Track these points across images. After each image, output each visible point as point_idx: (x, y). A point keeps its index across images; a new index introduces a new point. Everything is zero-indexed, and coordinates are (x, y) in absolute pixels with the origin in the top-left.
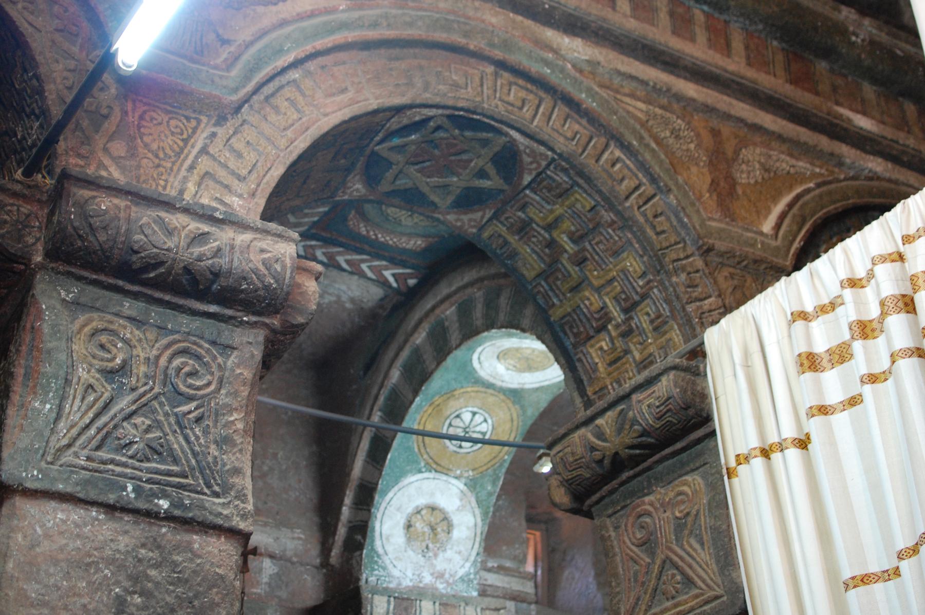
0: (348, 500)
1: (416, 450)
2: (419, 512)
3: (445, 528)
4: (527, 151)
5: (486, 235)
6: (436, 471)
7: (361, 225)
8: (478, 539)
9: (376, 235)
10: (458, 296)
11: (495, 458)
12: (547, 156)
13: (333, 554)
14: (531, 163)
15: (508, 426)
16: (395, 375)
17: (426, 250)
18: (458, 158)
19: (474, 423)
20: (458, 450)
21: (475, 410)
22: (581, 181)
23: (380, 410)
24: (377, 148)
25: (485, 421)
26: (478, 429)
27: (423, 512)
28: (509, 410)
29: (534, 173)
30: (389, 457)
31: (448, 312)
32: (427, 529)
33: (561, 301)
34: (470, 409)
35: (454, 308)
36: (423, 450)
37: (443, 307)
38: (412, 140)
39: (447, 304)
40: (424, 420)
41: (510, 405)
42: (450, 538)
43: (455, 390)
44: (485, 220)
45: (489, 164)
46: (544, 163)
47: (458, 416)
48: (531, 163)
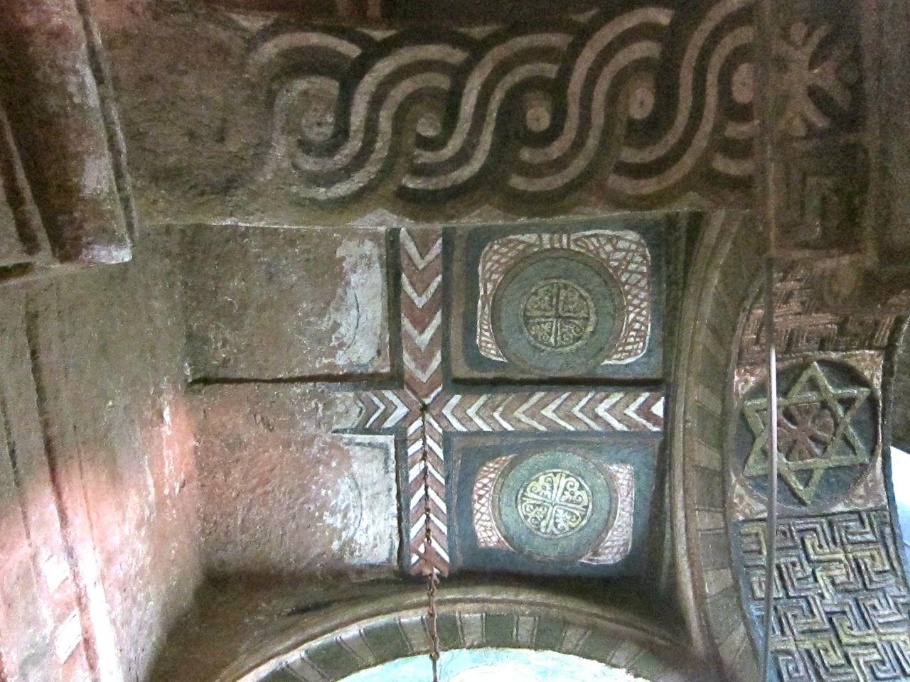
4: (870, 485)
5: (746, 529)
7: (492, 476)
9: (481, 497)
10: (500, 605)
12: (882, 500)
14: (861, 497)
16: (351, 632)
17: (489, 552)
18: (813, 444)
22: (889, 542)
23: (306, 651)
24: (815, 363)
29: (852, 508)
31: (467, 615)
33: (783, 632)
35: (479, 615)
37: (468, 606)
38: (826, 389)
39: (476, 606)
44: (759, 516)
45: (822, 471)
46: (871, 505)
48: (861, 497)
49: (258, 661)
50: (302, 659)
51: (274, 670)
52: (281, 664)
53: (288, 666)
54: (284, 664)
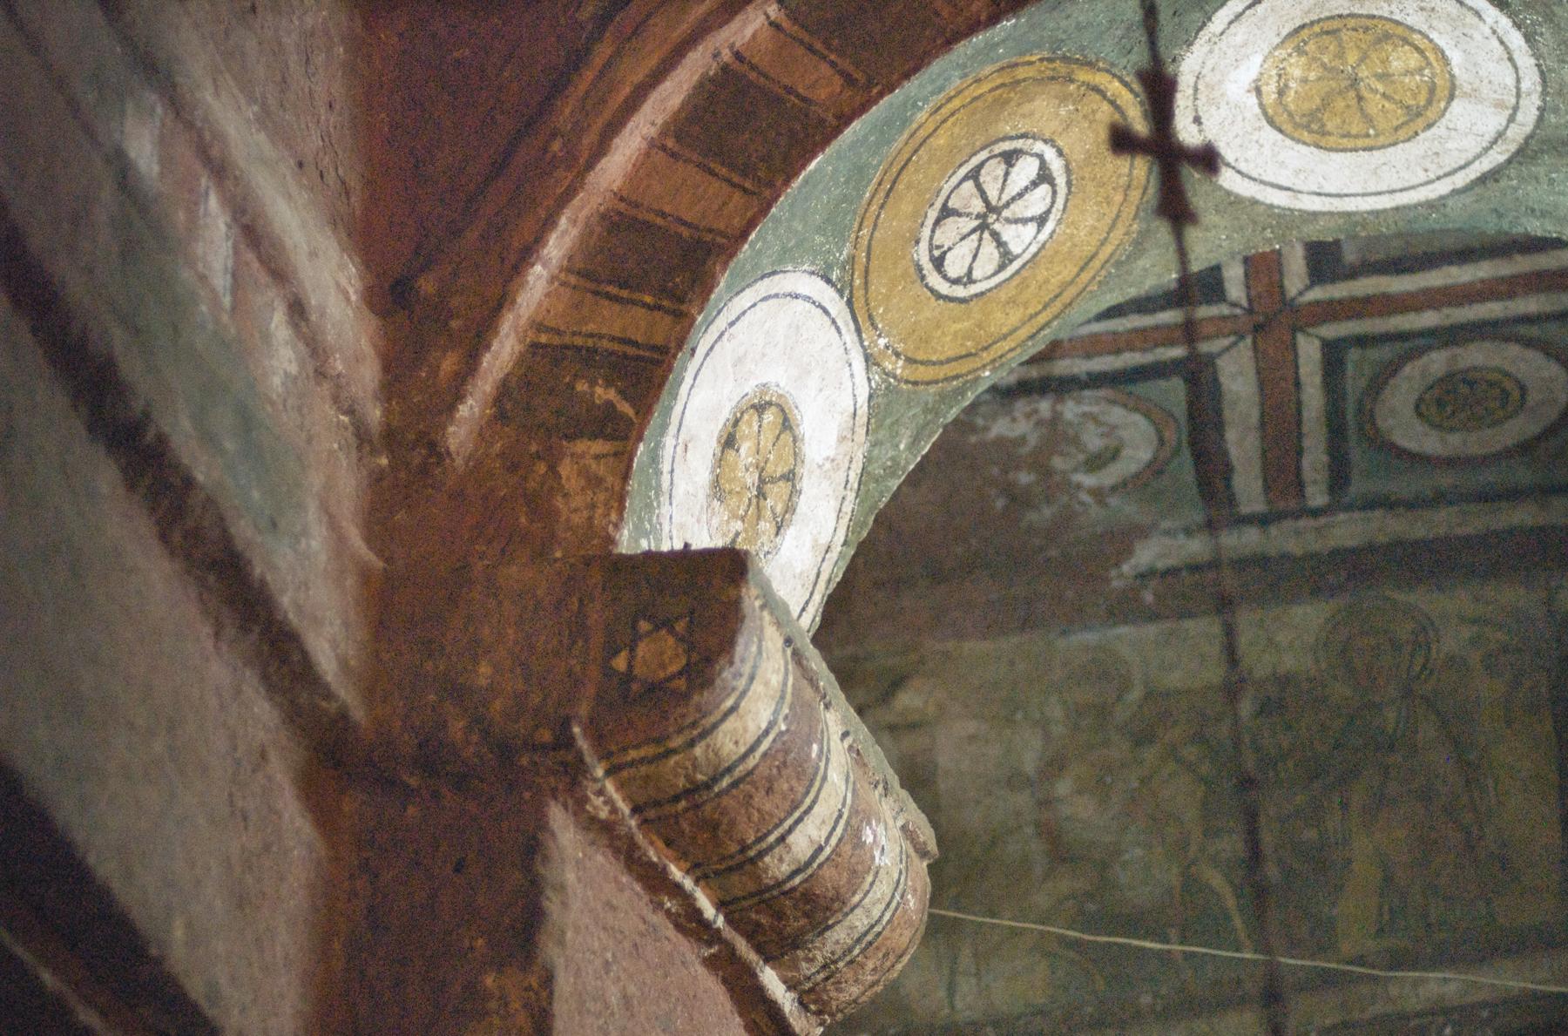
0: (557, 246)
1: (868, 195)
2: (760, 408)
3: (779, 509)
6: (850, 303)
8: (817, 598)
11: (969, 355)
13: (463, 410)
15: (1068, 272)
19: (1017, 209)
20: (928, 266)
21: (1056, 165)
25: (1041, 220)
26: (1008, 233)
27: (769, 416)
28: (1112, 227)
30: (812, 166)
32: (751, 479)
34: (1050, 154)
36: (874, 207)
40: (956, 103)
41: (1129, 211)
42: (777, 549)
43: (1090, 65)
47: (1010, 158)
49: (653, 62)
50: (775, 25)
51: (704, 76)
52: (716, 55)
53: (738, 56)
54: (726, 56)
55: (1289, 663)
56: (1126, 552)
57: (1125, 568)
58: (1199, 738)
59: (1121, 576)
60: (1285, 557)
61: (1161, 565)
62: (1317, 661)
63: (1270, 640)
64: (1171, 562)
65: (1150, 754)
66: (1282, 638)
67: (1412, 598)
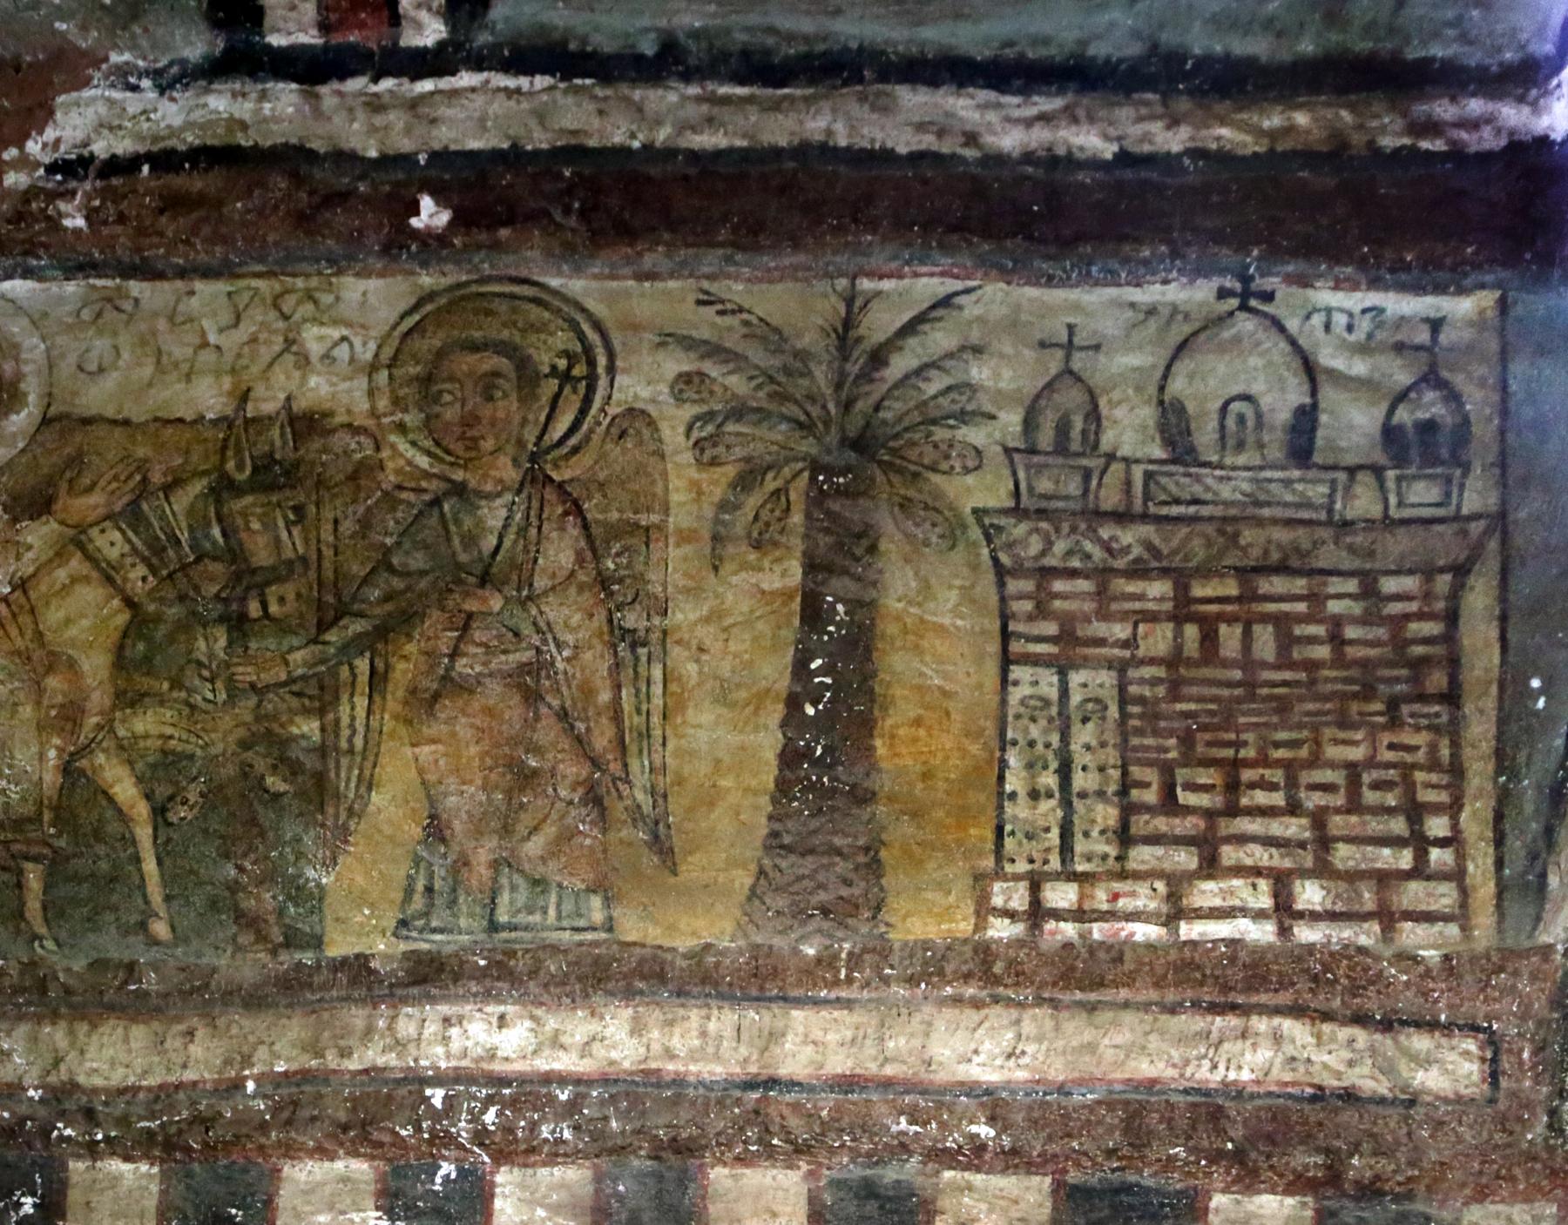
55: (318, 388)
56: (39, 114)
57: (33, 147)
58: (132, 516)
59: (25, 163)
60: (344, 158)
61: (100, 148)
62: (371, 393)
63: (289, 343)
64: (124, 146)
65: (38, 535)
66: (314, 338)
67: (576, 286)
